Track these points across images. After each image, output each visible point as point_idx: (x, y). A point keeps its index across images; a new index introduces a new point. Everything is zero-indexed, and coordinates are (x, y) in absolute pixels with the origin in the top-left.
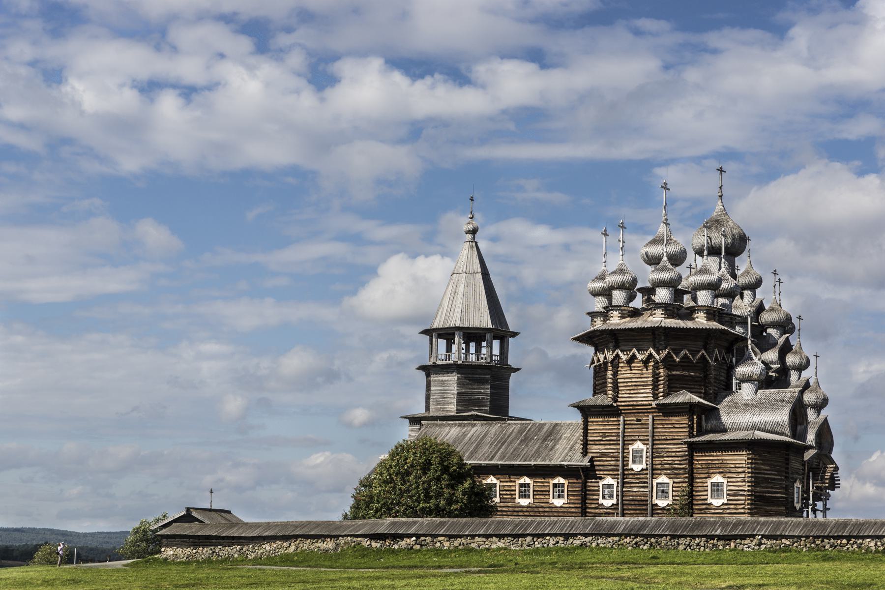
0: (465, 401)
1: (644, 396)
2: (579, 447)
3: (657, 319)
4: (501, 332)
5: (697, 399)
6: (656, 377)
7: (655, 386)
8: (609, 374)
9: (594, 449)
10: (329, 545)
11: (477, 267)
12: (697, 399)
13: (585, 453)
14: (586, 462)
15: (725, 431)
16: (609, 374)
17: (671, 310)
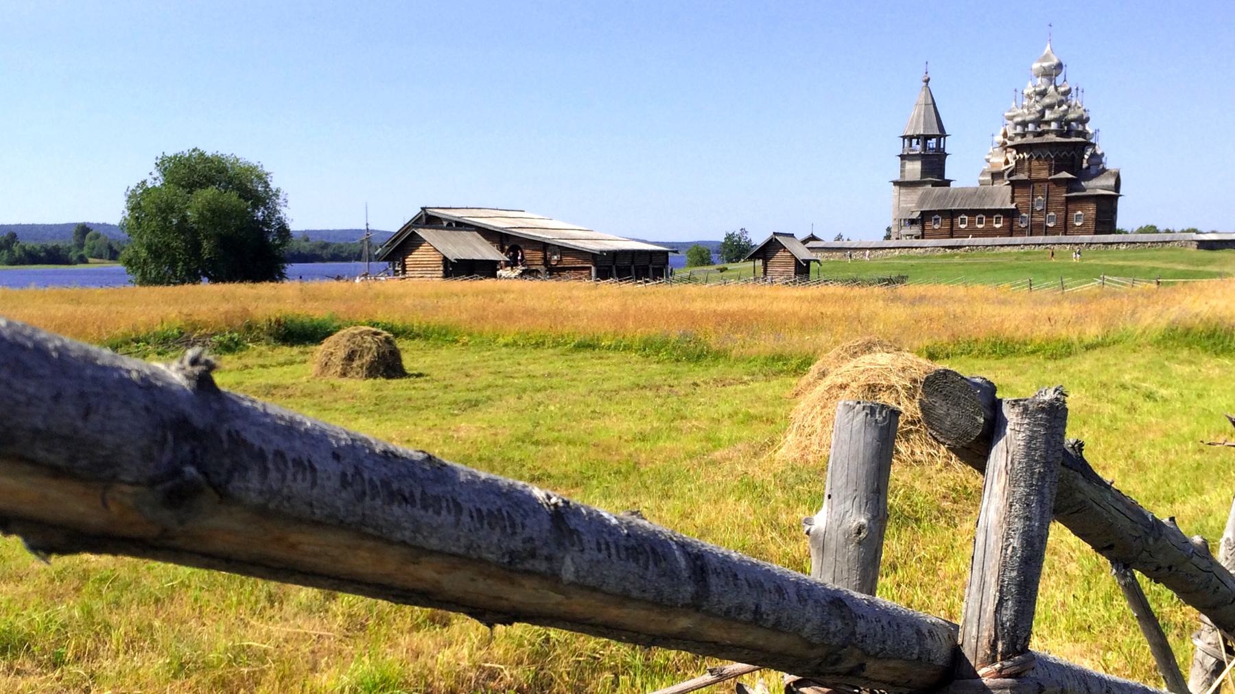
0: (924, 173)
1: (1044, 174)
2: (1008, 198)
3: (1052, 138)
4: (942, 134)
5: (1070, 176)
6: (1051, 165)
7: (1050, 170)
8: (1027, 164)
9: (1017, 200)
10: (922, 251)
11: (930, 101)
12: (1070, 176)
13: (1012, 202)
14: (1013, 206)
15: (1084, 190)
16: (1027, 164)
17: (1059, 133)
